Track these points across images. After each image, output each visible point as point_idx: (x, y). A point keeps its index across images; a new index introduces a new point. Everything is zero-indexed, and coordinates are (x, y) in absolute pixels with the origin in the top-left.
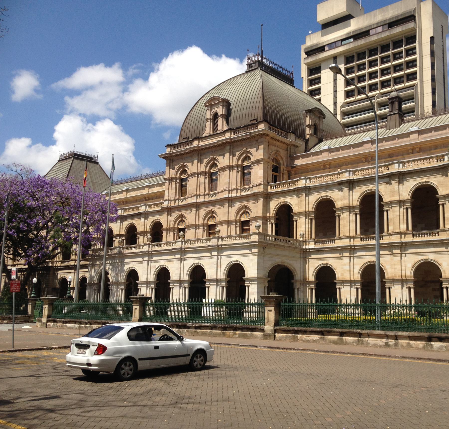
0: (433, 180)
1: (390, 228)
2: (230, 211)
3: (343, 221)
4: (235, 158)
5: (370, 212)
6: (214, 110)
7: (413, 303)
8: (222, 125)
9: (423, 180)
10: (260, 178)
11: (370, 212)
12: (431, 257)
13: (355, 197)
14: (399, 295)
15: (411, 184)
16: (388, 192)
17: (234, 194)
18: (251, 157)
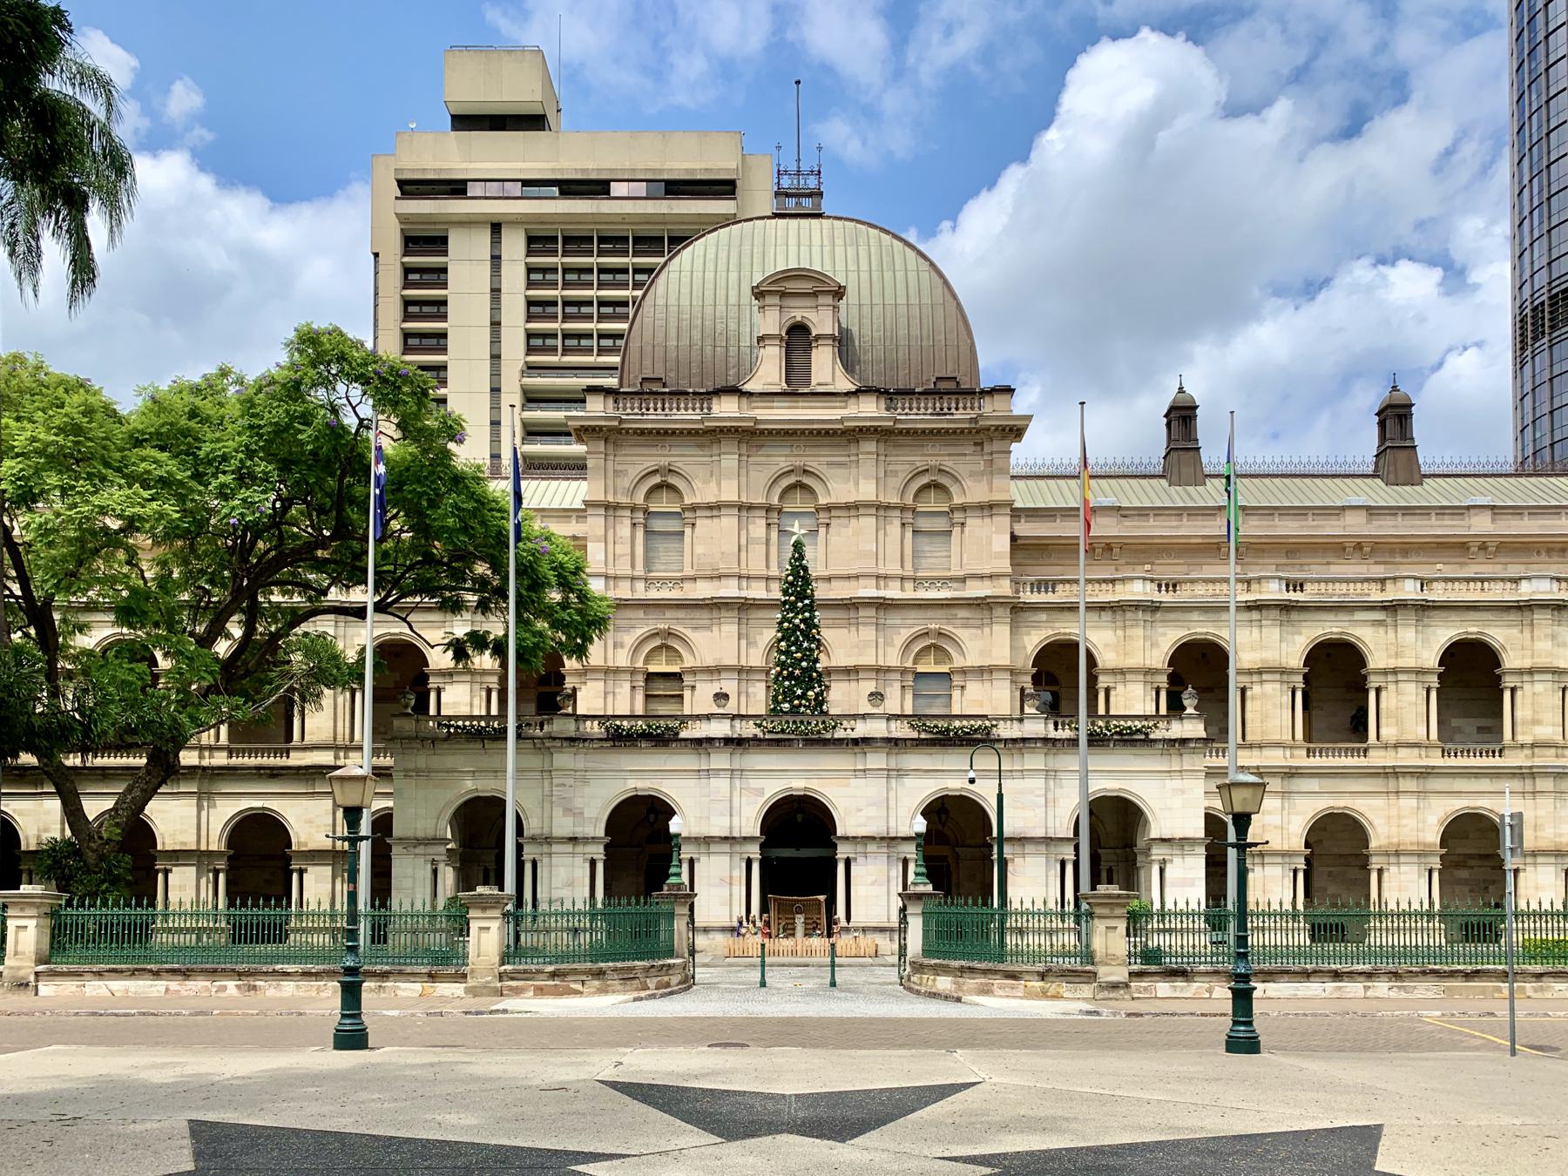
0: (1499, 634)
1: (1383, 731)
2: (881, 640)
3: (1257, 704)
4: (897, 482)
5: (1336, 688)
6: (798, 315)
7: (1437, 907)
8: (824, 367)
9: (1469, 627)
10: (998, 556)
11: (1336, 688)
12: (1484, 804)
13: (1290, 647)
14: (1405, 887)
15: (1444, 633)
16: (1382, 646)
17: (893, 592)
18: (954, 489)
